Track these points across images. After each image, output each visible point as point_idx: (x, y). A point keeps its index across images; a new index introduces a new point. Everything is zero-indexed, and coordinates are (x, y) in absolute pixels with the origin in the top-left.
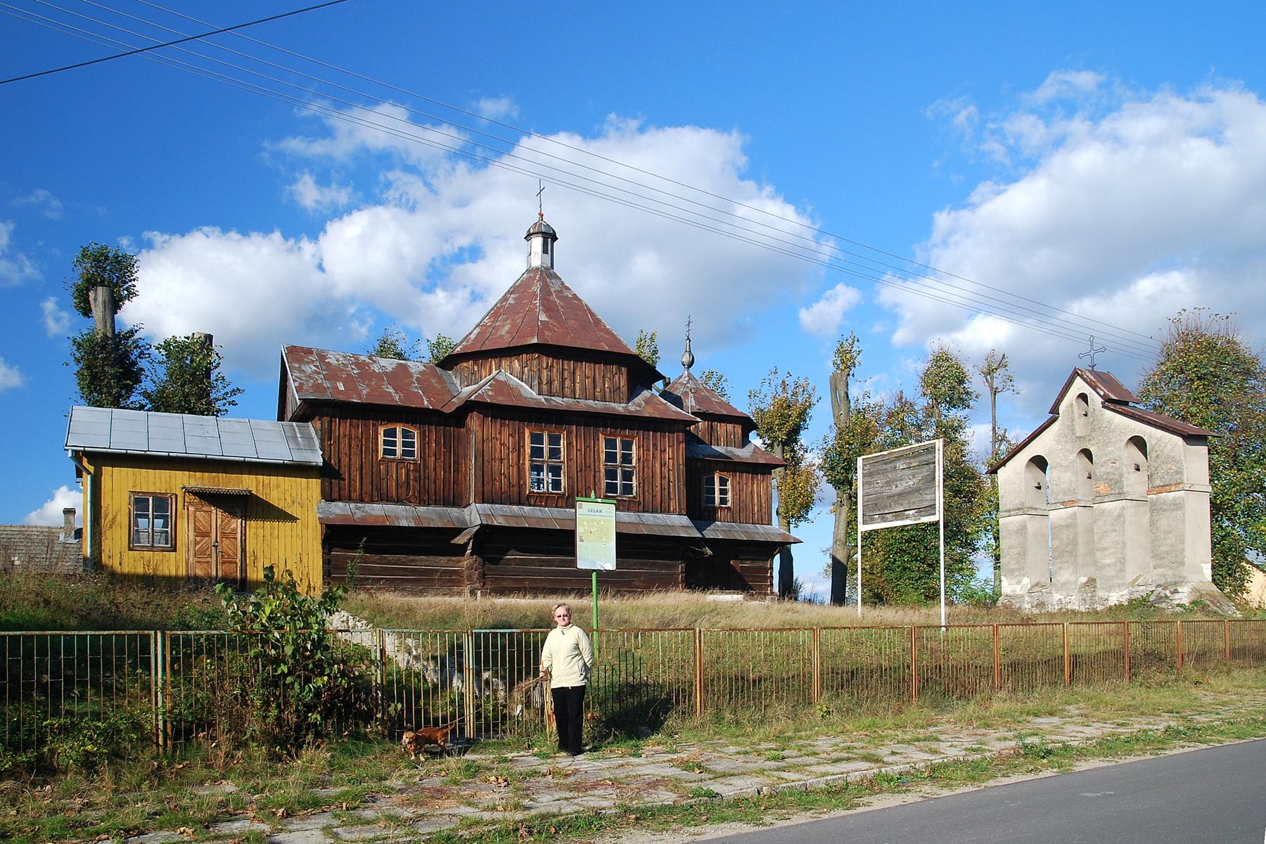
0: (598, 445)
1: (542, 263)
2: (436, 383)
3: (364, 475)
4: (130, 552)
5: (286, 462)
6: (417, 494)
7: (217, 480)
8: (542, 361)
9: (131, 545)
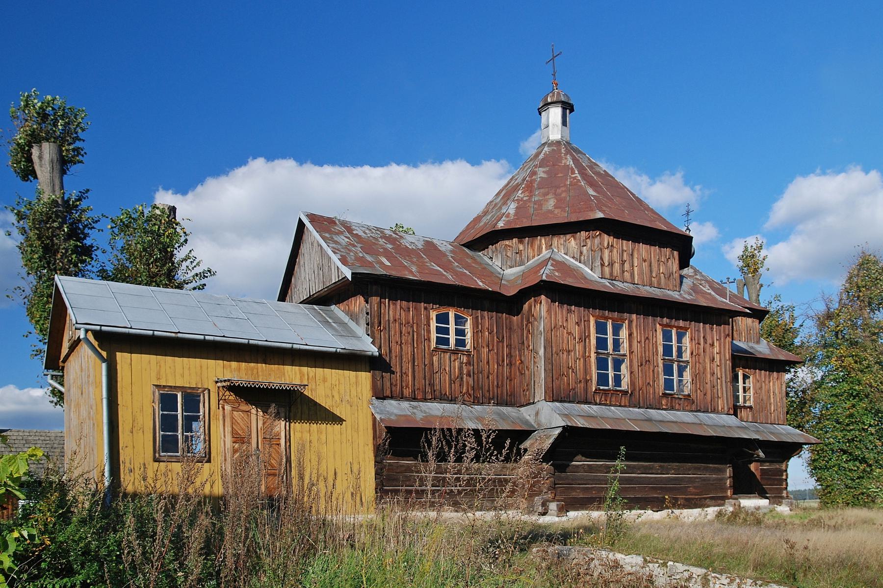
0: (656, 337)
1: (562, 137)
2: (473, 263)
3: (416, 368)
5: (338, 350)
6: (471, 392)
7: (255, 371)
8: (604, 239)
9: (157, 455)
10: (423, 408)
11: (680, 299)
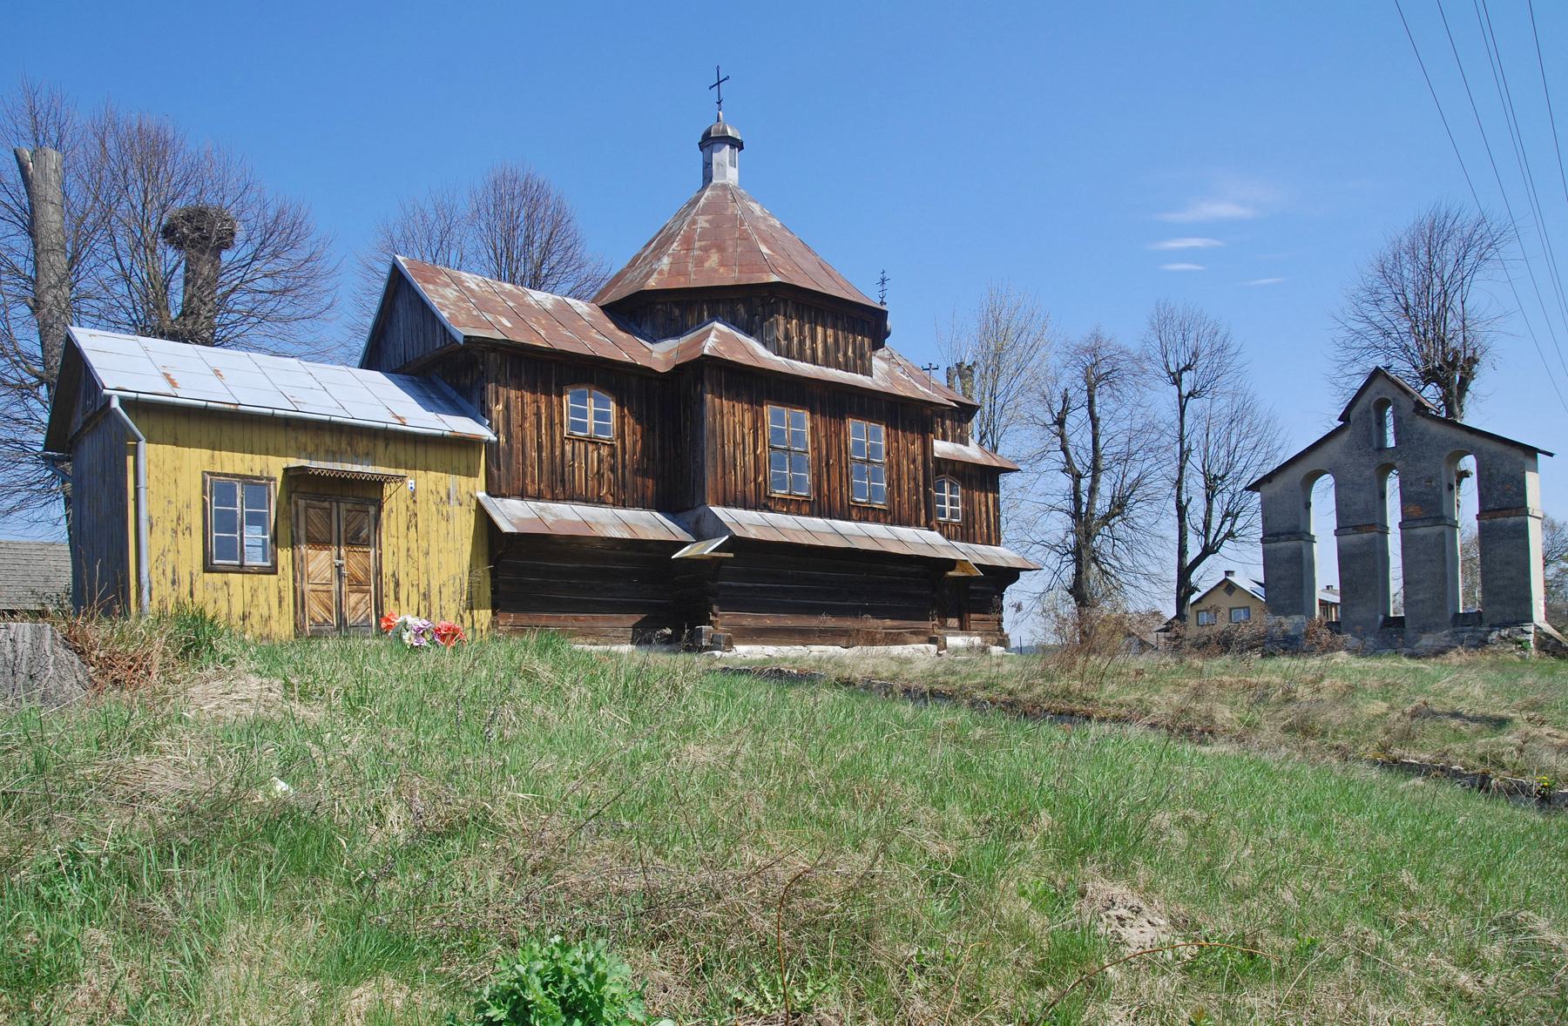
4: (206, 574)
5: (446, 433)
10: (554, 511)
11: (874, 387)
